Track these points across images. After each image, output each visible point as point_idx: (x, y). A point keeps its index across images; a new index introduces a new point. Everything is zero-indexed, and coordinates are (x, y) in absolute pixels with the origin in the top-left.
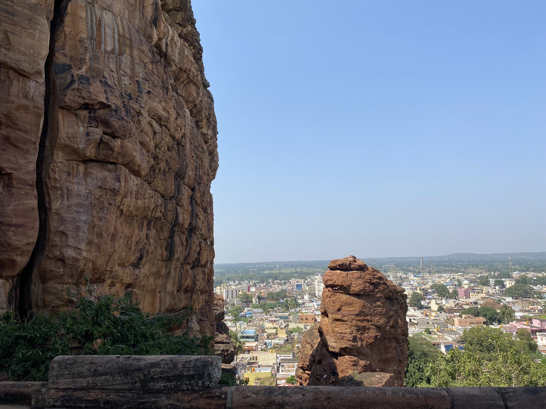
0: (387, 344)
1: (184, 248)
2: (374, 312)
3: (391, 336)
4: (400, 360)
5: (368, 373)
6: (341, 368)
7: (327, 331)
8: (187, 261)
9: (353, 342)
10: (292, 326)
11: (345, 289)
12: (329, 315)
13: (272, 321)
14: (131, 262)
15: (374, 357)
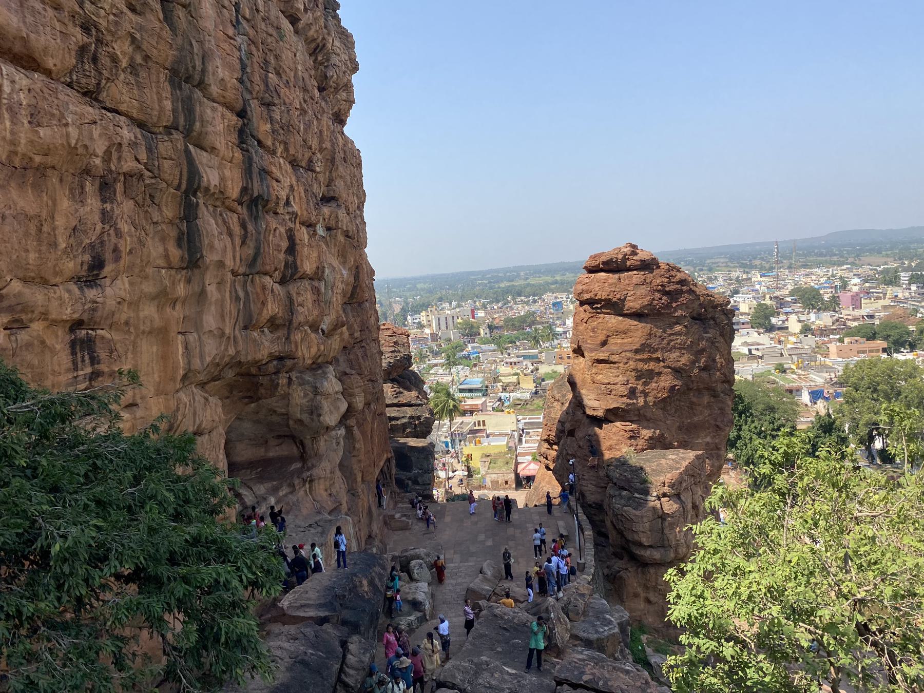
0: (694, 400)
1: (238, 241)
2: (669, 344)
3: (702, 386)
4: (717, 426)
5: (657, 452)
6: (608, 444)
7: (584, 380)
8: (258, 266)
9: (629, 397)
10: (544, 369)
11: (614, 306)
12: (586, 354)
13: (511, 364)
14: (68, 274)
15: (668, 422)
